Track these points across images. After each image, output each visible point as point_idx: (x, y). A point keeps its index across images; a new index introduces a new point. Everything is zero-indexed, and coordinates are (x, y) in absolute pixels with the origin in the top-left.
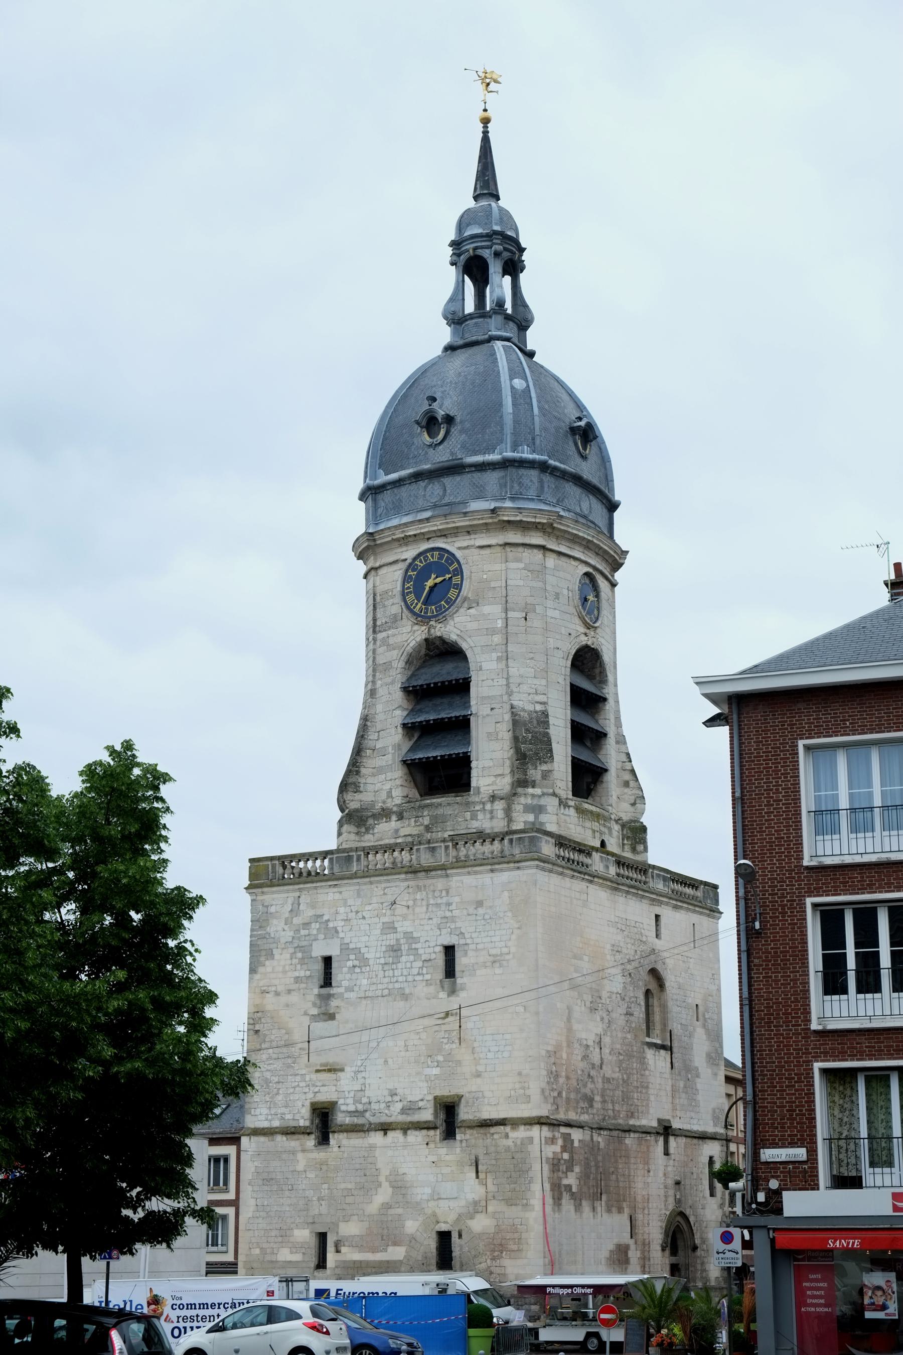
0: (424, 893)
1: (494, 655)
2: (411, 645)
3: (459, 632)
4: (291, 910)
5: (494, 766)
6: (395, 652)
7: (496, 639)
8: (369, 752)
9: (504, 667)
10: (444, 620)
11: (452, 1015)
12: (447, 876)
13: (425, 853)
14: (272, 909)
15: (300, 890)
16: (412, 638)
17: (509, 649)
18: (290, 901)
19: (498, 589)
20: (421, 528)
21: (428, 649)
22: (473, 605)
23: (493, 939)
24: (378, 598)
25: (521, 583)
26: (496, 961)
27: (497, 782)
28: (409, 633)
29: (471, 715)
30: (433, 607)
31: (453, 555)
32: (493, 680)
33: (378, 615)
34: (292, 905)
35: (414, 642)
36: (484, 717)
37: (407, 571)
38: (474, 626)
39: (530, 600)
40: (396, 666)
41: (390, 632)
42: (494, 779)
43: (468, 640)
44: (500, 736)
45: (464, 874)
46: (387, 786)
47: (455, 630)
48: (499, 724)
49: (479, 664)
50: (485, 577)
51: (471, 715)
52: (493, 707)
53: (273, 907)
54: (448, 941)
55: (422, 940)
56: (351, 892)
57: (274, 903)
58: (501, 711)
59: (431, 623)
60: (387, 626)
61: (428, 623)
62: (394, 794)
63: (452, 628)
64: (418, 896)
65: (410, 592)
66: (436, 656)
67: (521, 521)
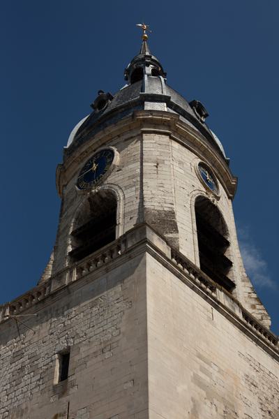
11: (60, 416)
23: (105, 327)
26: (106, 347)
54: (62, 346)
55: (42, 355)
67: (151, 119)
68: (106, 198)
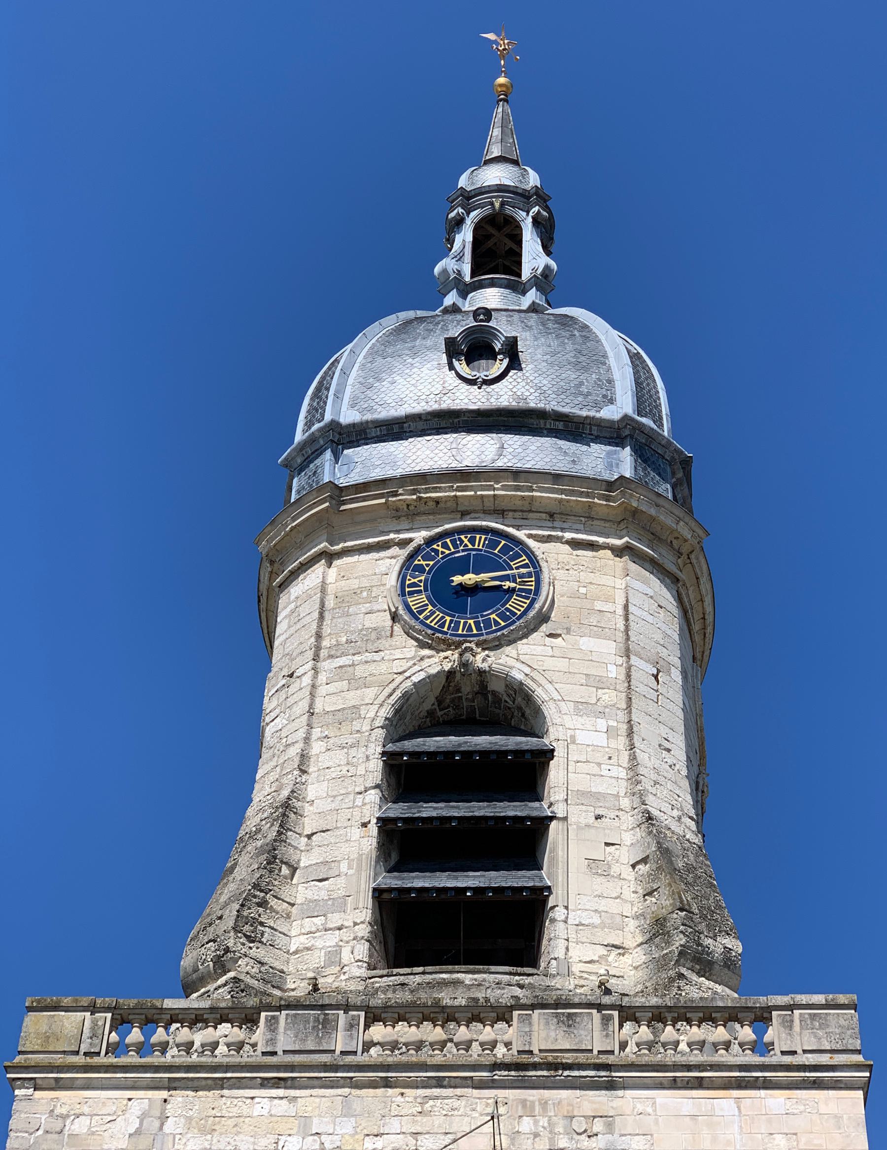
0: (544, 1122)
1: (602, 724)
2: (416, 679)
3: (527, 670)
4: (138, 1132)
5: (603, 926)
6: (370, 694)
7: (604, 697)
8: (285, 871)
9: (621, 747)
10: (496, 645)
12: (611, 1086)
13: (547, 1023)
14: (79, 1126)
15: (172, 1086)
16: (417, 668)
17: (634, 717)
18: (136, 1108)
19: (609, 615)
20: (459, 489)
21: (440, 701)
22: (559, 632)
24: (330, 603)
25: (650, 619)
27: (610, 959)
28: (408, 659)
29: (551, 818)
30: (471, 622)
31: (518, 542)
32: (599, 764)
33: (326, 630)
34: (142, 1118)
35: (422, 675)
36: (579, 828)
37: (411, 557)
38: (562, 664)
39: (664, 653)
40: (371, 714)
41: (357, 658)
42: (605, 953)
43: (548, 686)
44: (615, 869)
45: (660, 1086)
46: (331, 939)
47: (518, 665)
48: (613, 848)
49: (570, 732)
50: (583, 590)
51: (551, 818)
52: (600, 812)
53: (84, 1121)
56: (326, 1103)
57: (86, 1109)
58: (616, 823)
59: (468, 645)
60: (352, 646)
61: (459, 644)
62: (346, 956)
63: (511, 662)
64: (526, 1125)
65: (419, 592)
66: (445, 723)
68: (494, 693)
